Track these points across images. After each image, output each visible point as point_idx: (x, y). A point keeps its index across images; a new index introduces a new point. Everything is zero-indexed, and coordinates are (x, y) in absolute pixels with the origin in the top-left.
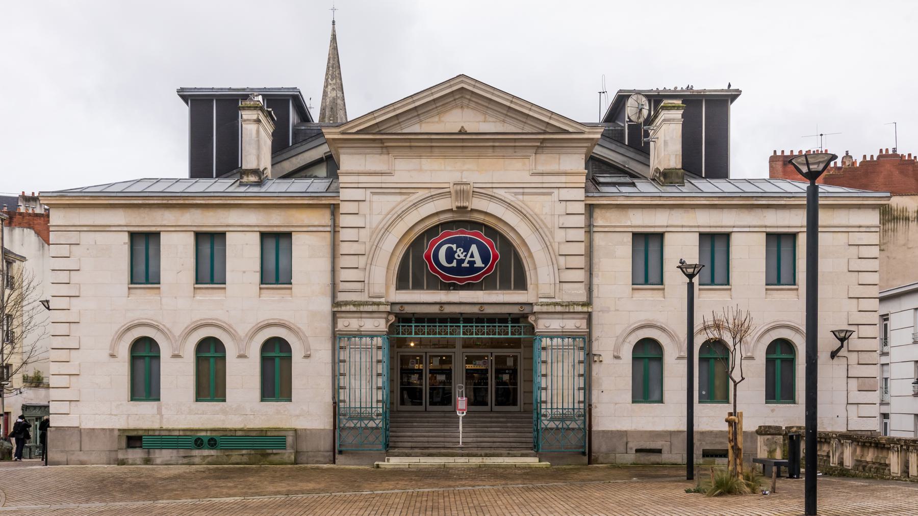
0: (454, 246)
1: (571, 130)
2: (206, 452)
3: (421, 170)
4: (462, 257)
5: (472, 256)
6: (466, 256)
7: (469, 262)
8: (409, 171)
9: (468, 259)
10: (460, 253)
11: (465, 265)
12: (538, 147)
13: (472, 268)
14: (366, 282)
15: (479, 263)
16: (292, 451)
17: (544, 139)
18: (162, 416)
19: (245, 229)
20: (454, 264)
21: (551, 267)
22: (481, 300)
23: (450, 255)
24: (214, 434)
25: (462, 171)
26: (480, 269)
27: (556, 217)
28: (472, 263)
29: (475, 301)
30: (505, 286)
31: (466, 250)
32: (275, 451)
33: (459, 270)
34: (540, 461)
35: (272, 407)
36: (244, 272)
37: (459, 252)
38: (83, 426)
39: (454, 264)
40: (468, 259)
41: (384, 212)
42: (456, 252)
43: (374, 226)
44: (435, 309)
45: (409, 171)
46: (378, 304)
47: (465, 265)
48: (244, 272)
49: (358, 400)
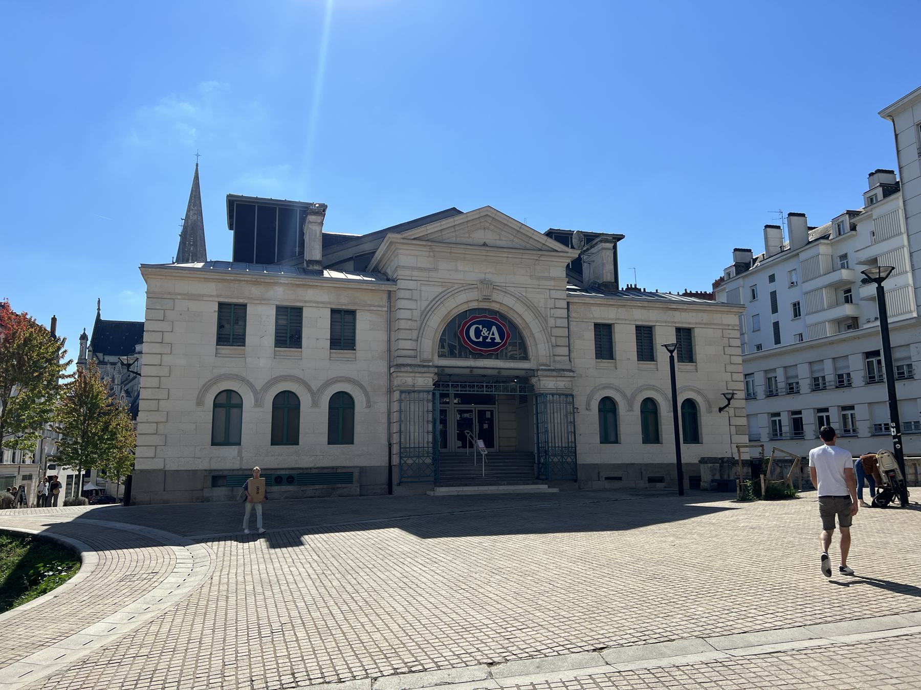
0: (481, 327)
1: (559, 250)
2: (284, 488)
3: (456, 270)
5: (493, 334)
6: (489, 334)
7: (491, 338)
8: (448, 270)
9: (490, 336)
10: (485, 332)
11: (489, 340)
12: (537, 260)
13: (493, 343)
14: (418, 350)
15: (498, 340)
17: (541, 255)
18: (242, 458)
19: (319, 304)
20: (481, 339)
21: (547, 344)
22: (499, 367)
23: (478, 333)
24: (291, 472)
25: (485, 274)
27: (549, 309)
29: (494, 366)
31: (489, 330)
32: (343, 485)
33: (484, 344)
34: (549, 487)
35: (337, 449)
36: (318, 339)
37: (484, 331)
38: (167, 468)
39: (481, 339)
40: (490, 336)
41: (430, 299)
42: (482, 331)
43: (423, 308)
45: (448, 270)
46: (429, 366)
47: (489, 340)
48: (318, 339)
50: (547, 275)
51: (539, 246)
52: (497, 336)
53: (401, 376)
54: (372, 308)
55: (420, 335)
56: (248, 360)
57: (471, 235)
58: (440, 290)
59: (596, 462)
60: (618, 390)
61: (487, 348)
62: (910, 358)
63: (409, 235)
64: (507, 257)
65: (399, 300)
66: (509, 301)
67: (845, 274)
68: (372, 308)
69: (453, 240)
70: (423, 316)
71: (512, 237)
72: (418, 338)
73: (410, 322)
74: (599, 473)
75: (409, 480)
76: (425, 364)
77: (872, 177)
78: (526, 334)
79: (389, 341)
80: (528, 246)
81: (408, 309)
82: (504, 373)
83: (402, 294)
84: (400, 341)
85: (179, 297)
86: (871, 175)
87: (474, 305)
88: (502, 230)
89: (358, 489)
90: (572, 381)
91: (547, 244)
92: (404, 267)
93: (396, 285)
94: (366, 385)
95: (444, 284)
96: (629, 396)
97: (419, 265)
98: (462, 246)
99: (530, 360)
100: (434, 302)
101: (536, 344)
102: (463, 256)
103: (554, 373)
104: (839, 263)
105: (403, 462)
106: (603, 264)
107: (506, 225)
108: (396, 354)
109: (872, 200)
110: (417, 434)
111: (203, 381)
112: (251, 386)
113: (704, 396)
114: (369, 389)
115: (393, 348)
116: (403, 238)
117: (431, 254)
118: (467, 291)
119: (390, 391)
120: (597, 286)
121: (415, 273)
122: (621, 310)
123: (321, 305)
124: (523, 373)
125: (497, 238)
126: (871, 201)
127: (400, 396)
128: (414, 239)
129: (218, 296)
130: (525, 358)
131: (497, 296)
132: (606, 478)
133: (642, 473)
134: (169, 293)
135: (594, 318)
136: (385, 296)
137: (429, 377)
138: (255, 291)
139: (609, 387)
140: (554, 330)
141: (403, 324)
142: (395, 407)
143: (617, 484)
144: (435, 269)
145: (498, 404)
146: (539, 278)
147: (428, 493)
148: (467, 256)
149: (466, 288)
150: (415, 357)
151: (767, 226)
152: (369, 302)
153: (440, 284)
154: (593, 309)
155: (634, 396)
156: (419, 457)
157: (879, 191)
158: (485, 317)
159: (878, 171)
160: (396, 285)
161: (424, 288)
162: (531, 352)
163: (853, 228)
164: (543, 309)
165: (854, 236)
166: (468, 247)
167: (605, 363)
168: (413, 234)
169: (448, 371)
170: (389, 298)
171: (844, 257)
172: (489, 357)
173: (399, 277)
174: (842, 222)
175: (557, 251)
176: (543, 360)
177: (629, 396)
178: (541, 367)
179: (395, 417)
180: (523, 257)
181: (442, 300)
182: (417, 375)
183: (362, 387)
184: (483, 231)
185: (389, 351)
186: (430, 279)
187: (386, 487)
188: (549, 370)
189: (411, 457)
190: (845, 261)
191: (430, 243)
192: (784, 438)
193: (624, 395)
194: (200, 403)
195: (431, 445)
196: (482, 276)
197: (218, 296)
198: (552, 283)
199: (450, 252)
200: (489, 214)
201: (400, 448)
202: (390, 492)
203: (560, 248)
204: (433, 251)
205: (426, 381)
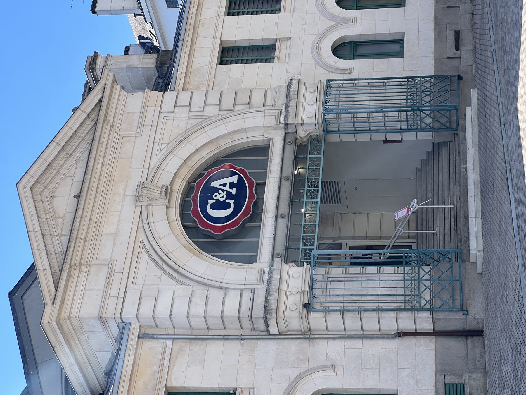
0: (210, 202)
1: (100, 96)
4: (224, 194)
5: (225, 185)
8: (114, 245)
9: (227, 188)
10: (220, 196)
12: (111, 127)
13: (240, 185)
14: (242, 287)
16: (466, 376)
17: (105, 119)
20: (232, 202)
21: (246, 115)
22: (278, 180)
23: (220, 206)
26: (240, 178)
27: (191, 114)
28: (232, 185)
29: (277, 185)
30: (264, 165)
31: (217, 190)
33: (239, 198)
34: (469, 105)
40: (227, 188)
41: (159, 272)
42: (217, 200)
44: (282, 223)
45: (114, 245)
46: (271, 271)
47: (234, 191)
49: (393, 284)
51: (89, 124)
52: (228, 180)
53: (285, 311)
54: (166, 363)
55: (218, 284)
57: (61, 215)
58: (145, 258)
59: (432, 62)
60: (323, 36)
63: (50, 293)
64: (103, 164)
65: (157, 314)
68: (166, 363)
69: (65, 239)
70: (187, 281)
71: (72, 160)
72: (221, 288)
73: (194, 300)
74: (448, 58)
75: (458, 297)
76: (266, 277)
78: (226, 144)
79: (225, 338)
80: (89, 139)
83: (146, 310)
84: (225, 314)
87: (175, 214)
88: (58, 172)
89: (474, 375)
90: (305, 84)
91: (88, 111)
92: (102, 307)
93: (130, 324)
94: (296, 373)
95: (136, 252)
96: (331, 23)
97: (101, 287)
98: (78, 220)
99: (269, 140)
100: (165, 266)
101: (245, 130)
102: (92, 225)
103: (293, 103)
105: (428, 306)
106: (129, 68)
107: (49, 165)
108: (246, 324)
110: (382, 284)
114: (304, 368)
115: (234, 330)
116: (54, 302)
117: (84, 268)
118: (150, 219)
120: (161, 81)
121: (114, 292)
122: (201, 31)
124: (290, 150)
125: (69, 180)
127: (318, 311)
128: (56, 287)
131: (164, 179)
132: (457, 48)
133: (448, 7)
135: (211, 64)
137: (289, 271)
139: (317, 47)
140: (224, 106)
141: (198, 310)
143: (466, 37)
144: (110, 265)
145: (340, 238)
146: (141, 125)
147: (479, 269)
148: (94, 218)
149: (145, 221)
150: (254, 291)
151: (93, 11)
152: (156, 368)
153: (135, 258)
154: (196, 64)
155: (332, 17)
156: (420, 280)
158: (196, 195)
160: (130, 324)
161: (140, 281)
164: (191, 121)
166: (80, 213)
167: (281, 51)
168: (49, 288)
169: (280, 248)
170: (152, 337)
172: (262, 186)
173: (118, 315)
175: (100, 101)
176: (271, 120)
177: (331, 23)
178: (282, 121)
180: (105, 143)
181: (161, 254)
182: (284, 287)
183: (299, 378)
184: (56, 200)
185: (241, 338)
186: (127, 271)
187: (470, 340)
188: (287, 111)
189: (420, 293)
191: (67, 266)
193: (330, 29)
195: (401, 269)
196: (129, 200)
198: (151, 109)
199: (85, 240)
200: (30, 185)
201: (404, 310)
202: (478, 333)
203: (97, 94)
204: (80, 265)
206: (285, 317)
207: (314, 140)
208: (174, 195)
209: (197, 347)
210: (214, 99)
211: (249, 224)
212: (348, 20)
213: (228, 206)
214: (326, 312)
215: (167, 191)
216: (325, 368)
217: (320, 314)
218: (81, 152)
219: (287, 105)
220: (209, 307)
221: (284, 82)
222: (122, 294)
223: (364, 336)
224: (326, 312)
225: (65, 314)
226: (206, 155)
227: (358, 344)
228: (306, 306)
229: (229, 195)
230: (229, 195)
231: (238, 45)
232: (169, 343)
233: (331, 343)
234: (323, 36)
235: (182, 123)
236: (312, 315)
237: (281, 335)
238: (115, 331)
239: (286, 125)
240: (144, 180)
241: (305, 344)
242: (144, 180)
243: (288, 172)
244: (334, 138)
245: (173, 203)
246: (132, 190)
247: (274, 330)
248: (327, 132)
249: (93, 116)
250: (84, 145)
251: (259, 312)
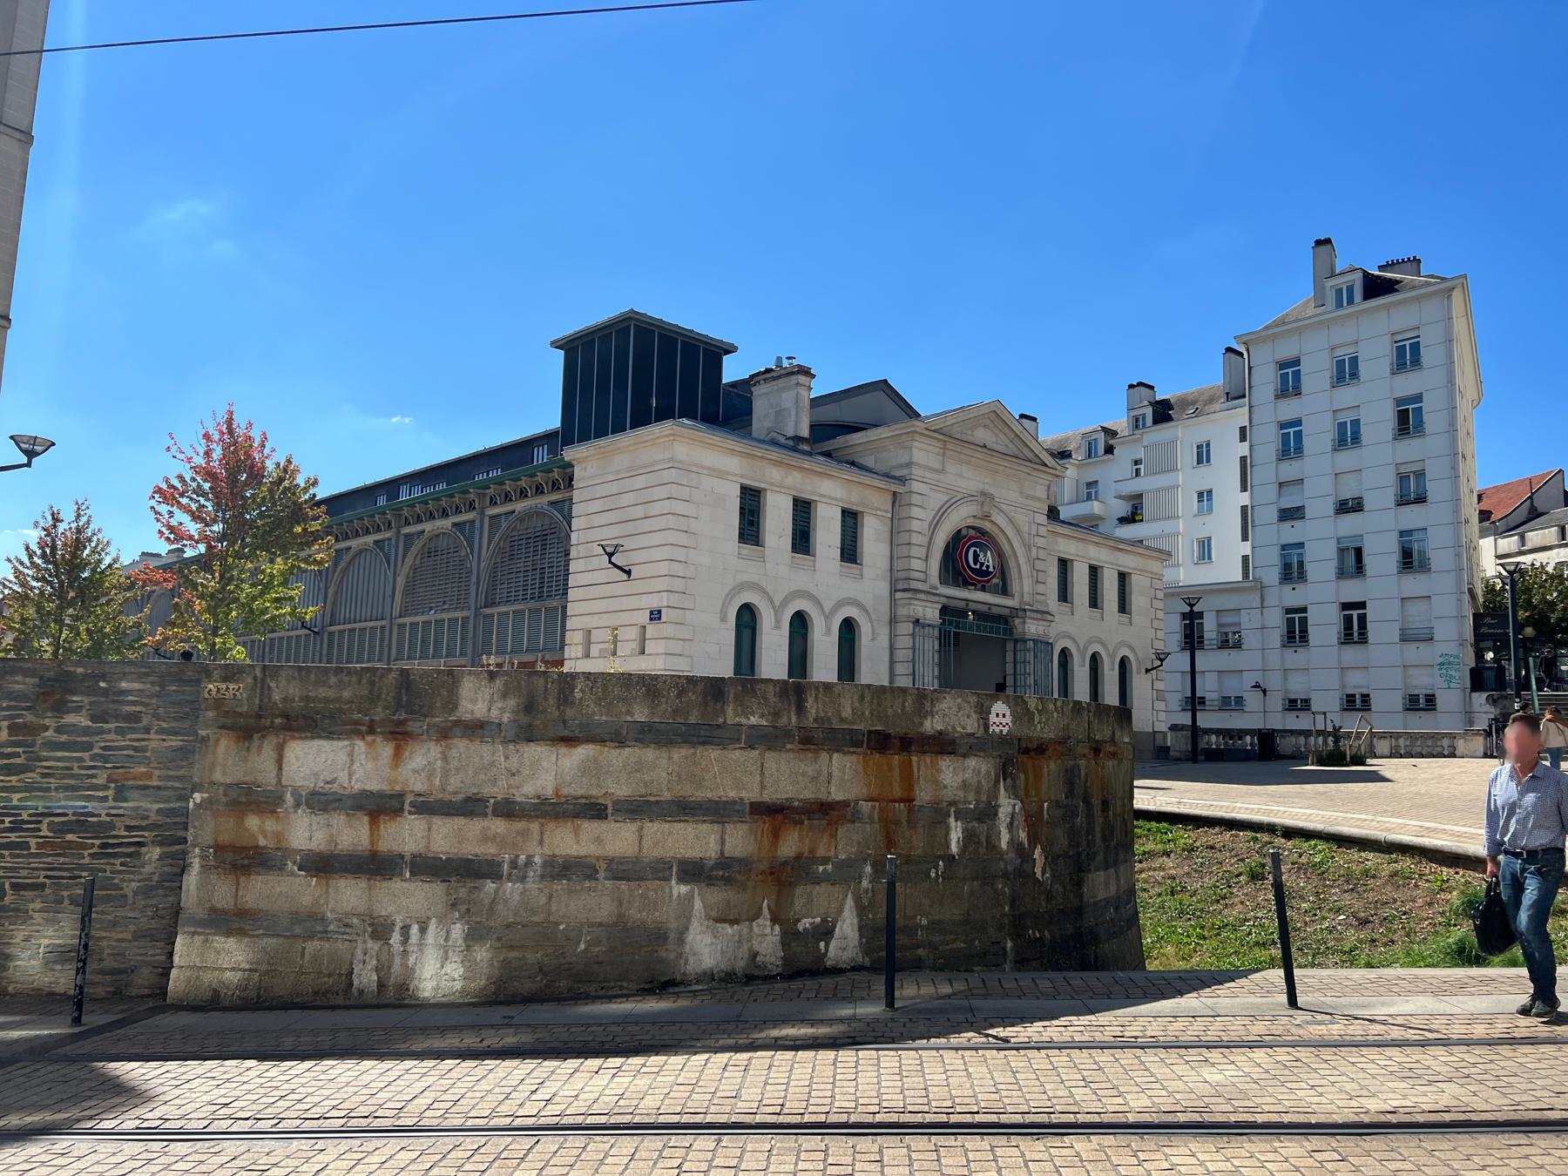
3: (961, 476)
11: (984, 568)
13: (987, 573)
20: (978, 566)
23: (976, 556)
28: (988, 567)
33: (979, 572)
50: (1032, 493)
51: (1031, 456)
52: (991, 563)
54: (879, 513)
56: (768, 565)
58: (946, 498)
60: (1074, 641)
61: (979, 578)
62: (1239, 624)
65: (913, 507)
66: (1000, 520)
67: (1096, 507)
68: (879, 513)
69: (958, 436)
71: (1007, 441)
73: (920, 536)
77: (1132, 390)
78: (1012, 563)
80: (1021, 455)
81: (919, 518)
82: (995, 610)
84: (912, 560)
85: (705, 472)
86: (1131, 386)
87: (970, 522)
94: (871, 611)
97: (931, 464)
99: (1013, 596)
101: (1021, 578)
103: (1039, 616)
104: (1086, 491)
108: (902, 575)
109: (1137, 420)
111: (727, 589)
112: (771, 601)
113: (1136, 654)
114: (873, 617)
116: (927, 429)
119: (893, 621)
121: (928, 474)
122: (1081, 545)
123: (834, 502)
124: (1005, 612)
126: (1137, 423)
128: (935, 431)
129: (742, 476)
130: (1005, 591)
134: (696, 465)
135: (1059, 552)
136: (889, 498)
138: (775, 474)
142: (904, 642)
144: (942, 471)
146: (1029, 497)
150: (925, 581)
154: (1060, 540)
155: (1086, 648)
157: (1149, 412)
159: (1140, 384)
161: (932, 494)
162: (1015, 586)
163: (1109, 450)
165: (1109, 460)
171: (1090, 485)
173: (913, 477)
174: (1095, 439)
175: (1046, 465)
176: (1027, 598)
179: (902, 655)
182: (929, 604)
186: (939, 484)
188: (1033, 611)
190: (1093, 491)
192: (1207, 708)
194: (723, 619)
196: (981, 486)
197: (742, 476)
204: (944, 449)
205: (932, 614)
206: (910, 604)
207: (1009, 631)
208: (981, 522)
209: (887, 535)
210: (1042, 554)
211: (960, 578)
212: (1084, 661)
213: (976, 564)
214: (913, 635)
215: (987, 517)
216: (873, 633)
217: (911, 632)
218: (1012, 449)
219: (1037, 611)
220: (917, 547)
221: (1051, 610)
222: (925, 480)
223: (892, 662)
224: (913, 635)
225: (917, 437)
226: (1006, 547)
227: (886, 658)
228: (918, 620)
229: (982, 564)
230: (982, 564)
231: (1069, 574)
232: (889, 515)
233: (887, 638)
234: (1074, 641)
235: (1026, 529)
236: (911, 625)
237: (893, 600)
238: (898, 473)
239: (1025, 610)
240: (997, 500)
241: (887, 618)
242: (997, 500)
243: (973, 606)
244: (1010, 646)
245: (978, 521)
246: (991, 490)
247: (899, 595)
248: (1016, 641)
249: (1037, 460)
250: (1016, 452)
251: (914, 585)
